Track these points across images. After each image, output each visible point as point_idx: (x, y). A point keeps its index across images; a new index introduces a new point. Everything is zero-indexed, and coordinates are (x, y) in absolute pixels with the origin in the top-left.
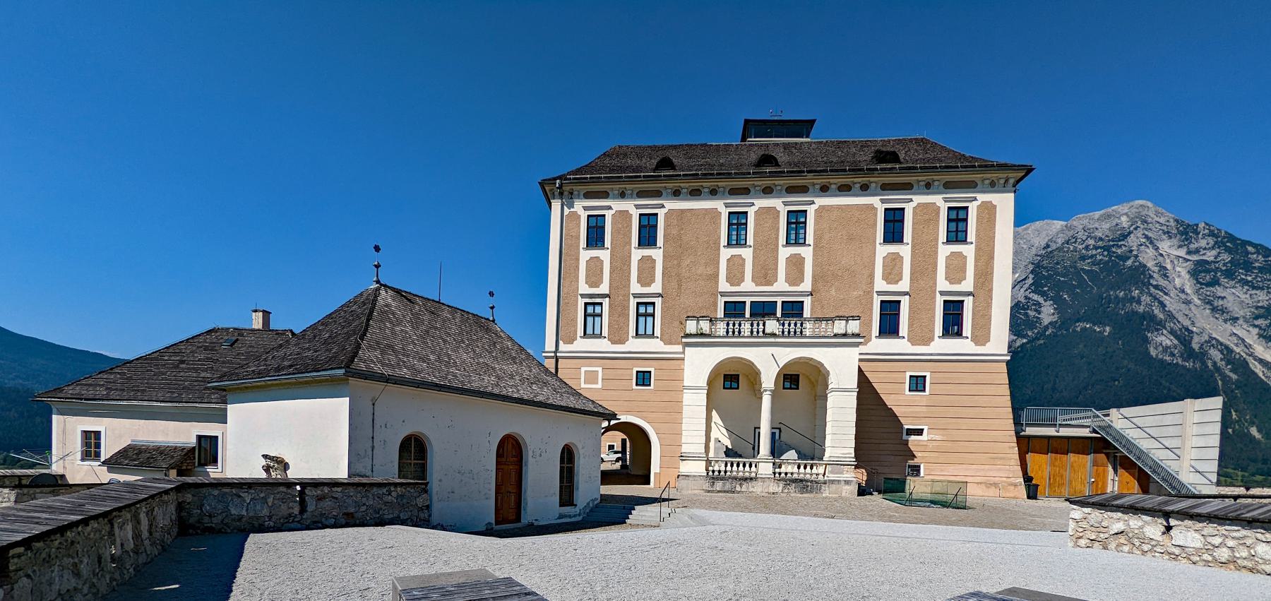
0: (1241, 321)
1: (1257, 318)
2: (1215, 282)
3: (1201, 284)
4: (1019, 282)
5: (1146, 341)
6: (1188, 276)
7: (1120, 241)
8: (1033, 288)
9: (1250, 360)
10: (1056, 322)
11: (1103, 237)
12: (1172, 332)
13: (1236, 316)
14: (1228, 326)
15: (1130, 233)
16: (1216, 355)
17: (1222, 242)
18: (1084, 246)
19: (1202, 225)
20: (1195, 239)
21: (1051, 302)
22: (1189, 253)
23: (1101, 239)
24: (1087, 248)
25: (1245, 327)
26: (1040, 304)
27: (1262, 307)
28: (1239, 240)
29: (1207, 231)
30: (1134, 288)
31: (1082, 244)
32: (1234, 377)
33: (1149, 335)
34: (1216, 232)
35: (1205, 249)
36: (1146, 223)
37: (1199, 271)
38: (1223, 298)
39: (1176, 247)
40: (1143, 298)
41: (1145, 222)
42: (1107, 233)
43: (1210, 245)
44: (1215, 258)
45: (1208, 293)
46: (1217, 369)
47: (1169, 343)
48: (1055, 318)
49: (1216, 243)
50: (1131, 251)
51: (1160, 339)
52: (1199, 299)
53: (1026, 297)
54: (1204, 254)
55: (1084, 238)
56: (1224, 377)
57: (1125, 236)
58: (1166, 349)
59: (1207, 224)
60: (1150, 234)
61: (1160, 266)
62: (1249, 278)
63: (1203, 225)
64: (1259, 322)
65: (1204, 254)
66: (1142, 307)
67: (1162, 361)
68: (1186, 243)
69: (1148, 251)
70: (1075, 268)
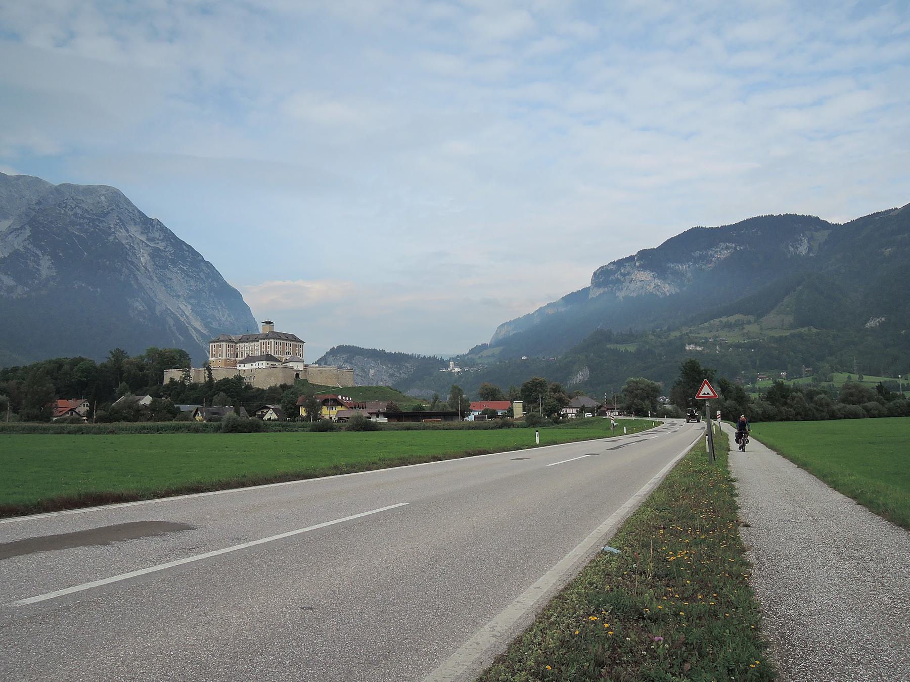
0: (181, 299)
1: (190, 297)
2: (164, 267)
3: (157, 265)
4: (16, 229)
6: (149, 258)
7: (101, 217)
8: (31, 240)
9: (190, 328)
11: (89, 210)
13: (179, 294)
15: (108, 213)
16: (171, 322)
18: (72, 213)
22: (148, 240)
24: (76, 215)
25: (184, 303)
26: (38, 256)
29: (159, 227)
30: (116, 261)
32: (182, 339)
35: (158, 239)
37: (155, 254)
42: (92, 207)
44: (165, 248)
45: (162, 274)
51: (137, 304)
52: (156, 277)
53: (25, 247)
54: (158, 243)
55: (73, 206)
57: (105, 215)
60: (122, 218)
61: (130, 245)
62: (185, 268)
64: (192, 301)
65: (158, 243)
68: (146, 231)
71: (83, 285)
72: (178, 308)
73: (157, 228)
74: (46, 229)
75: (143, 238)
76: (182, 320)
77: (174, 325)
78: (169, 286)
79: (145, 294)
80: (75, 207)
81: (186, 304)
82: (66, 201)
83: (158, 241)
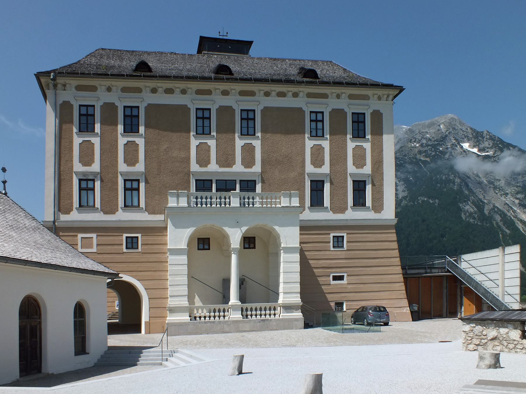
0: (509, 196)
1: (518, 193)
5: (460, 210)
10: (407, 197)
11: (431, 138)
12: (473, 203)
13: (507, 192)
14: (503, 198)
16: (498, 218)
17: (496, 144)
19: (485, 132)
20: (482, 141)
21: (403, 182)
23: (430, 140)
27: (519, 186)
28: (505, 142)
30: (450, 173)
31: (419, 143)
32: (508, 231)
33: (461, 205)
34: (493, 137)
35: (488, 148)
36: (454, 129)
38: (499, 180)
39: (472, 146)
40: (456, 180)
41: (454, 129)
42: (433, 135)
43: (490, 146)
45: (491, 177)
46: (499, 227)
47: (472, 211)
48: (405, 194)
49: (493, 144)
50: (447, 148)
51: (467, 207)
52: (487, 181)
55: (420, 138)
56: (503, 231)
58: (471, 214)
59: (488, 132)
60: (457, 138)
63: (486, 132)
64: (519, 196)
66: (456, 186)
67: (469, 223)
68: (478, 144)
69: (457, 148)
70: (416, 159)
71: (426, 199)
72: (504, 205)
73: (486, 138)
74: (401, 162)
75: (475, 150)
76: (509, 214)
77: (501, 221)
78: (498, 187)
79: (474, 197)
80: (421, 139)
81: (513, 200)
82: (415, 136)
83: (488, 150)
